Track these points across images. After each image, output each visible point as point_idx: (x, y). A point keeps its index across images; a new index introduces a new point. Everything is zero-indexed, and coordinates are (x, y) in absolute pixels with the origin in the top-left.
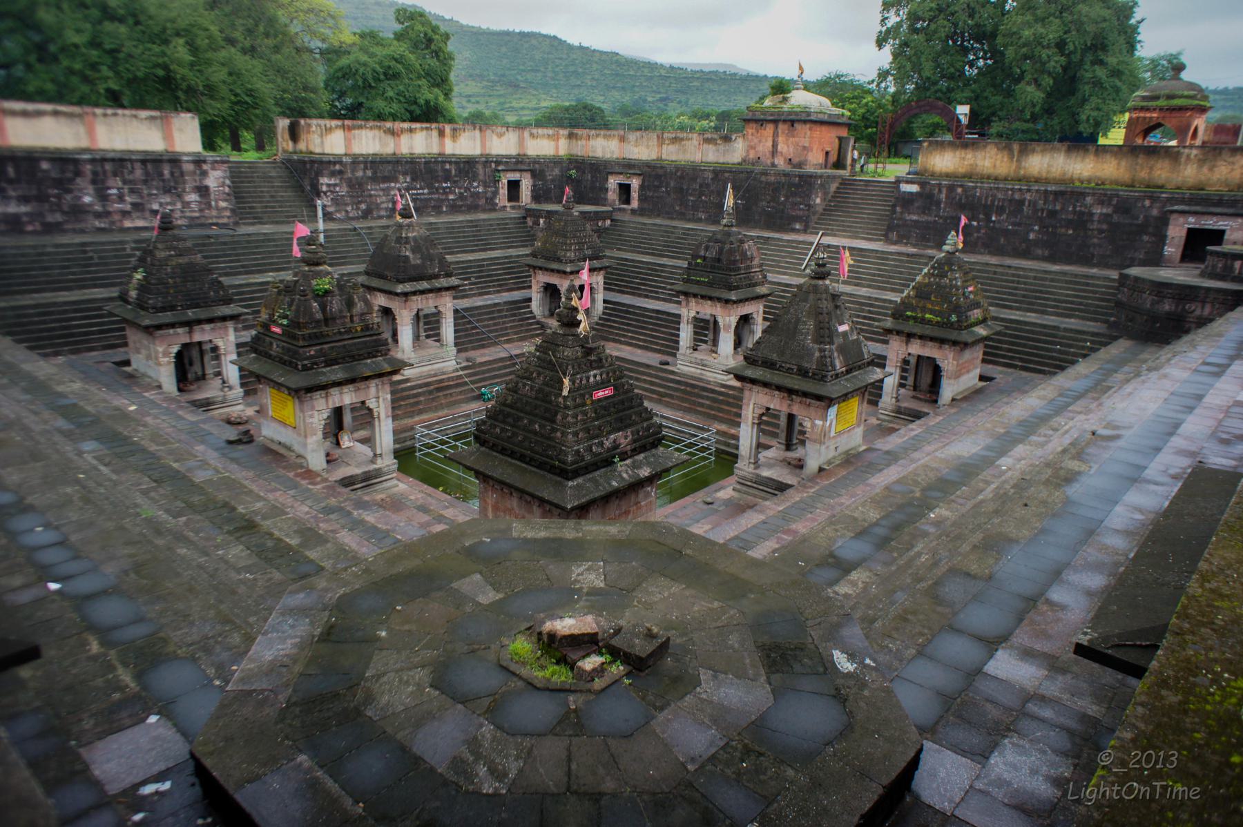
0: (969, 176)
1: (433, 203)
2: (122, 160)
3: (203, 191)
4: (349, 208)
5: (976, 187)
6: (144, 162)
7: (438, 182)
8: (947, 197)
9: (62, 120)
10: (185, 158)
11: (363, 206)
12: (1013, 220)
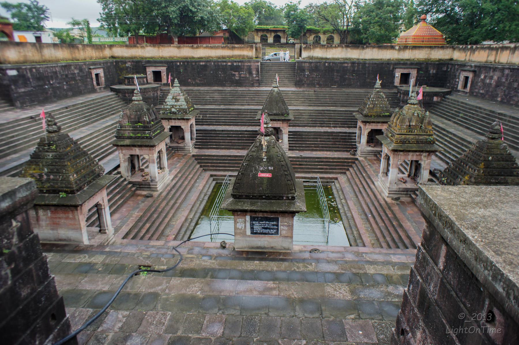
0: (25, 62)
5: (40, 68)
8: (31, 75)
12: (57, 81)
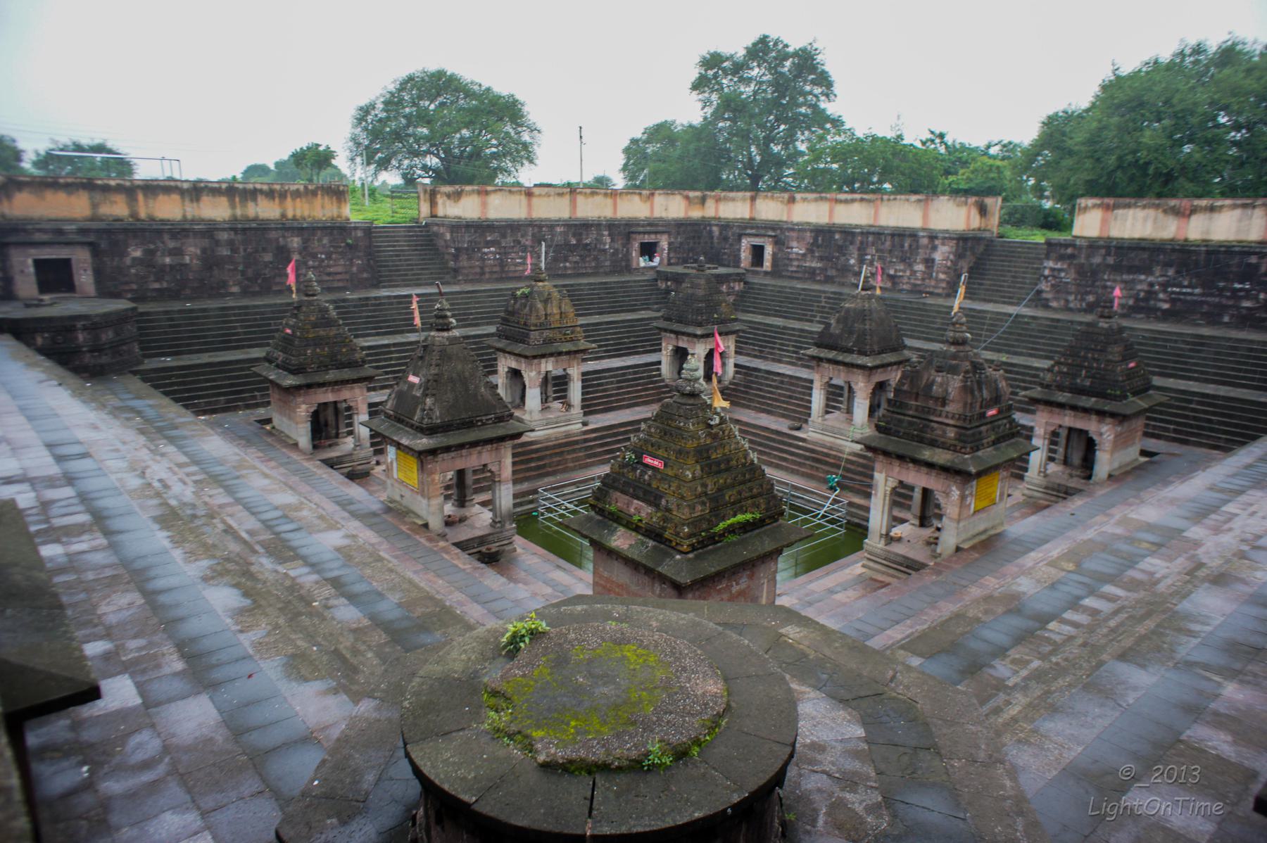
1: (1205, 308)
2: (879, 234)
3: (929, 262)
4: (1071, 298)
6: (893, 235)
7: (1226, 280)
9: (864, 204)
10: (921, 234)
11: (1091, 298)
